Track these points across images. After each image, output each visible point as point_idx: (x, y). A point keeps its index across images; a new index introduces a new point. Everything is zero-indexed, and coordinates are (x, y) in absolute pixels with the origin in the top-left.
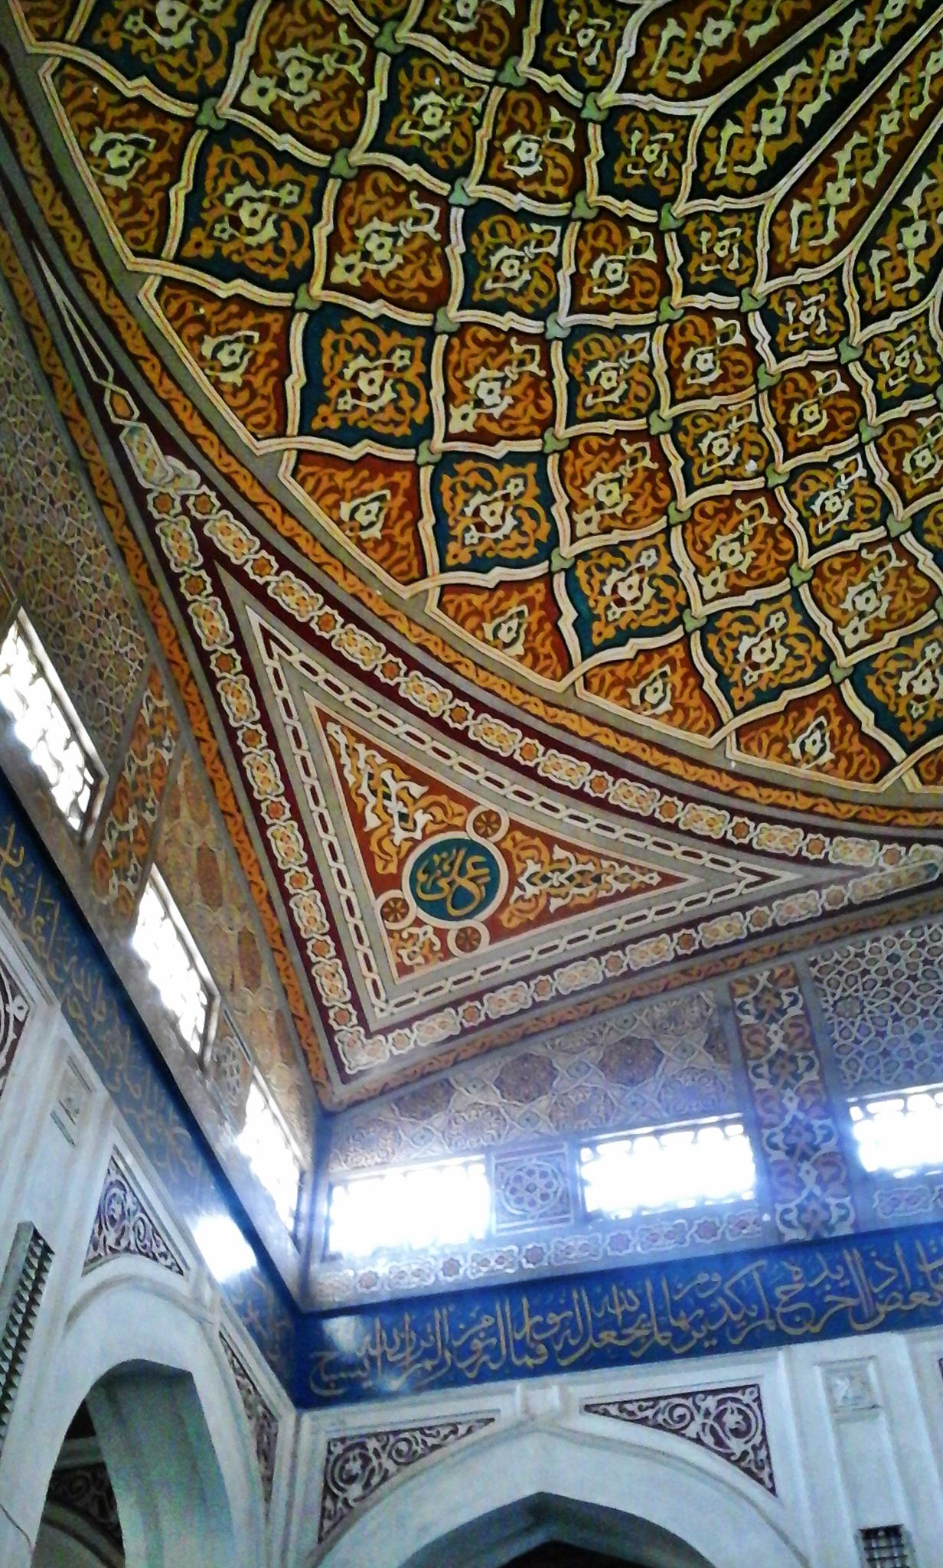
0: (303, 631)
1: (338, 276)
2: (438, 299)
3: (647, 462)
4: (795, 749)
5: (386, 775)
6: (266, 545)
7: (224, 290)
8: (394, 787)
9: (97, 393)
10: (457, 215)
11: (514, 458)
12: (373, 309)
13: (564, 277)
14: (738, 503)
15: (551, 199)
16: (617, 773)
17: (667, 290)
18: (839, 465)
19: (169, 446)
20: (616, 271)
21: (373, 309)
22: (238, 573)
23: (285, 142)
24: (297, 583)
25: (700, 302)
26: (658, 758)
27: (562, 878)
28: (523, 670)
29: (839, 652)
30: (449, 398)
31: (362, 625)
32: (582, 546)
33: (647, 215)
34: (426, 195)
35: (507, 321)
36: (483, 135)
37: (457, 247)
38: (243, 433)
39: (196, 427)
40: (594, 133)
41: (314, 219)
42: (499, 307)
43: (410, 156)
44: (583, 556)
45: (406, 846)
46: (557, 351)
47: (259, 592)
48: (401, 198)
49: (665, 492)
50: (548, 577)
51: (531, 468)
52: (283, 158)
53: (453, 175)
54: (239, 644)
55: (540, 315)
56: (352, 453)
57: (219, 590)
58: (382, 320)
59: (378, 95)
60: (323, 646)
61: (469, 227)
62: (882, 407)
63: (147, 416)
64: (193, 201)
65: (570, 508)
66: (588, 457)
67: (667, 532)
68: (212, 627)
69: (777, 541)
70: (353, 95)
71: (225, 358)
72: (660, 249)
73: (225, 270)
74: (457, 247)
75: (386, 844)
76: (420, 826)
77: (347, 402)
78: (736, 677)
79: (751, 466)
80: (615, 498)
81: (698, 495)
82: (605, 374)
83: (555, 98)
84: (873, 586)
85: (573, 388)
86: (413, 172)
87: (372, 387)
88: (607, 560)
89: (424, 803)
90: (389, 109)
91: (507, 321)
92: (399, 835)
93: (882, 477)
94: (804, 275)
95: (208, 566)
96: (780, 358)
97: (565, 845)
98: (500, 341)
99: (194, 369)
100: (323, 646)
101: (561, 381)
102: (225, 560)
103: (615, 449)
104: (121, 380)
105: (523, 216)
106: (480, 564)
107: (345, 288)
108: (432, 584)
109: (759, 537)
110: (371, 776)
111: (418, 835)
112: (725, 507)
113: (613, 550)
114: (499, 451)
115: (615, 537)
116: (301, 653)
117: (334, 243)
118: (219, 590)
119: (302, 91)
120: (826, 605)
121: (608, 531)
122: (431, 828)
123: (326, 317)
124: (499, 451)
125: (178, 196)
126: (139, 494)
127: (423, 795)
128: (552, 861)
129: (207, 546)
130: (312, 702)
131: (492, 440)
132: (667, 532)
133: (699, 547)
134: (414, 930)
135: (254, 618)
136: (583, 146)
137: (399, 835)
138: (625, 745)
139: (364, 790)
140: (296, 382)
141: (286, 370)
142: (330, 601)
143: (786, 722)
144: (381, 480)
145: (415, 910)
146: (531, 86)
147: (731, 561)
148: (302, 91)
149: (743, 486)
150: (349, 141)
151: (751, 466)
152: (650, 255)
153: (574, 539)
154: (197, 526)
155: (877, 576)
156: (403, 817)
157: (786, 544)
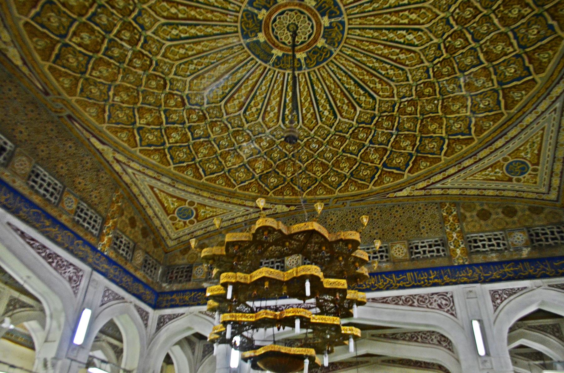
0: (444, 179)
2: (386, 150)
7: (376, 178)
8: (487, 173)
11: (420, 141)
12: (385, 158)
13: (386, 131)
15: (371, 132)
16: (505, 134)
17: (393, 115)
19: (401, 190)
21: (385, 158)
22: (428, 186)
23: (354, 167)
25: (396, 109)
26: (505, 126)
28: (469, 146)
32: (444, 132)
33: (377, 118)
34: (367, 149)
35: (392, 140)
36: (358, 141)
37: (377, 146)
40: (361, 125)
42: (389, 141)
43: (360, 151)
44: (446, 133)
47: (433, 183)
48: (367, 153)
50: (449, 139)
52: (357, 168)
54: (442, 189)
55: (392, 135)
56: (411, 165)
57: (431, 189)
58: (387, 157)
59: (349, 155)
60: (449, 176)
62: (429, 77)
63: (395, 192)
67: (446, 118)
68: (437, 192)
70: (348, 159)
73: (374, 177)
74: (377, 146)
80: (435, 126)
81: (439, 111)
82: (407, 126)
83: (353, 131)
85: (408, 131)
86: (362, 151)
87: (400, 160)
88: (449, 129)
90: (351, 153)
91: (392, 140)
93: (447, 78)
94: (395, 91)
96: (412, 96)
97: (521, 147)
98: (396, 141)
99: (390, 184)
100: (449, 176)
101: (406, 133)
103: (424, 125)
105: (373, 136)
108: (443, 157)
112: (444, 107)
113: (447, 127)
114: (418, 143)
115: (444, 127)
116: (449, 180)
117: (372, 163)
118: (431, 189)
119: (347, 165)
121: (442, 128)
123: (385, 165)
124: (418, 143)
125: (360, 182)
126: (408, 196)
130: (461, 180)
131: (415, 144)
132: (446, 118)
133: (453, 112)
135: (438, 185)
136: (363, 127)
138: (498, 132)
140: (395, 171)
141: (393, 172)
142: (440, 173)
145: (521, 177)
146: (351, 134)
147: (458, 107)
148: (347, 165)
149: (440, 103)
151: (436, 102)
154: (417, 190)
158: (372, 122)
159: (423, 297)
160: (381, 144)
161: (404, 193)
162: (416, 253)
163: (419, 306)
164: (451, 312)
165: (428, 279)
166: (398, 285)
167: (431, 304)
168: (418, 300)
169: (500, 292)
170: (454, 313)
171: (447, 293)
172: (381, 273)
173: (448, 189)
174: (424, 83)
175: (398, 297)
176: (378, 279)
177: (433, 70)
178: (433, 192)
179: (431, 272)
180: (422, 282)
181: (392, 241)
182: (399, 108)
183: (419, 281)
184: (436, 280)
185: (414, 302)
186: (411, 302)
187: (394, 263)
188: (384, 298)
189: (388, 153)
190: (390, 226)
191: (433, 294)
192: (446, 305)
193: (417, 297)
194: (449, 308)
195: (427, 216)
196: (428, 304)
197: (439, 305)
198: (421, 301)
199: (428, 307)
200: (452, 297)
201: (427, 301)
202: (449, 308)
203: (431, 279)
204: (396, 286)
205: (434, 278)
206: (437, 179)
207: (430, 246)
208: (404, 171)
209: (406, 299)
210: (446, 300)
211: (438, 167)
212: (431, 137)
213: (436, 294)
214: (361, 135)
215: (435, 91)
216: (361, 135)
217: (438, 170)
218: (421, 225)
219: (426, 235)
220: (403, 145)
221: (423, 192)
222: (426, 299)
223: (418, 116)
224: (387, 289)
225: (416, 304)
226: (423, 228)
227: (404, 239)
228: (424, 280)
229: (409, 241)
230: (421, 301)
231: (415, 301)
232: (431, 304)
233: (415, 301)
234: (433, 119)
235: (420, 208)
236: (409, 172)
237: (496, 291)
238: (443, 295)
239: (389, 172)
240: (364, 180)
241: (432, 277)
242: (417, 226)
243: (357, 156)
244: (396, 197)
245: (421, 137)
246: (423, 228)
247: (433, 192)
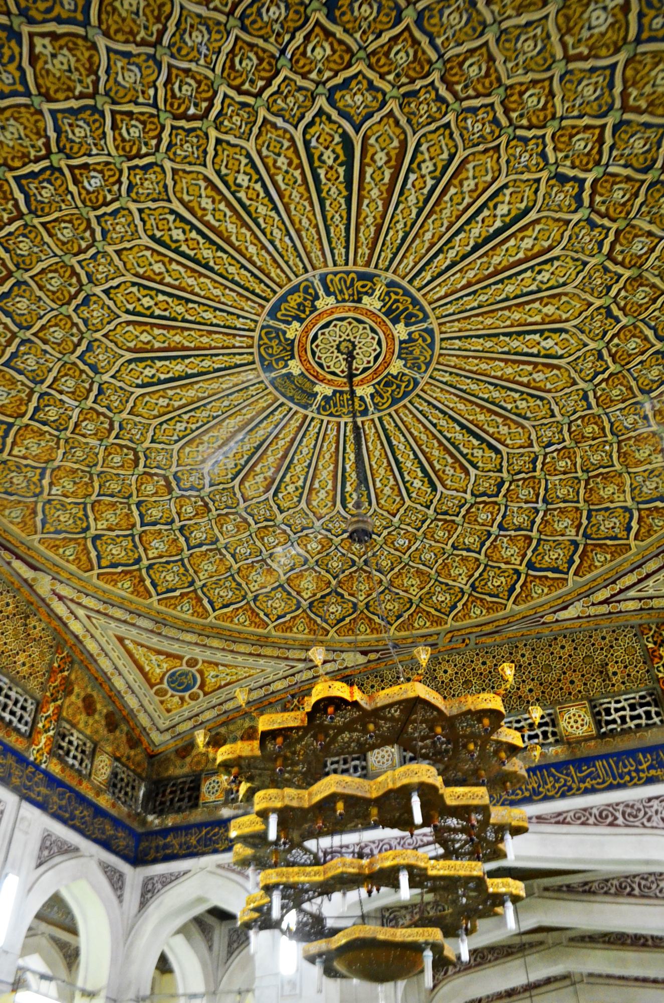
0: (640, 581)
1: (518, 562)
3: (599, 480)
6: (606, 587)
7: (518, 590)
9: (544, 623)
10: (502, 533)
11: (589, 517)
15: (499, 510)
17: (534, 477)
19: (565, 608)
20: (525, 492)
21: (529, 553)
22: (613, 596)
23: (477, 574)
24: (622, 580)
25: (539, 465)
30: (563, 535)
31: (644, 563)
33: (507, 485)
34: (495, 540)
35: (538, 520)
36: (478, 527)
37: (513, 533)
38: (564, 589)
39: (560, 601)
40: (479, 500)
41: (499, 568)
42: (533, 522)
43: (483, 544)
44: (633, 499)
46: (550, 507)
47: (621, 591)
49: (612, 474)
50: (639, 510)
51: (594, 513)
52: (481, 575)
53: (489, 534)
54: (640, 599)
55: (537, 511)
56: (577, 561)
57: (619, 602)
58: (533, 552)
59: (465, 553)
60: (648, 576)
61: (506, 530)
62: (590, 407)
63: (555, 612)
64: (491, 595)
65: (612, 502)
68: (632, 605)
70: (464, 559)
71: (540, 591)
72: (519, 480)
74: (513, 533)
77: (559, 562)
79: (607, 448)
80: (611, 489)
81: (616, 462)
82: (562, 492)
83: (468, 511)
85: (565, 501)
86: (488, 544)
88: (637, 492)
90: (468, 550)
91: (538, 520)
94: (533, 437)
95: (609, 604)
96: (564, 441)
98: (545, 522)
100: (648, 576)
101: (562, 505)
102: (607, 599)
103: (591, 489)
104: (542, 617)
105: (504, 517)
106: (629, 529)
107: (522, 561)
108: (633, 544)
113: (632, 490)
114: (585, 522)
115: (628, 489)
117: (507, 563)
118: (619, 602)
119: (463, 570)
121: (624, 491)
123: (530, 566)
124: (585, 522)
125: (489, 599)
126: (579, 617)
129: (601, 603)
131: (580, 524)
132: (629, 473)
133: (639, 463)
135: (632, 593)
136: (484, 502)
140: (550, 575)
141: (546, 577)
146: (464, 517)
147: (648, 452)
148: (463, 570)
149: (615, 449)
150: (477, 560)
151: (607, 448)
152: (520, 483)
153: (625, 501)
154: (593, 604)
158: (499, 491)
159: (632, 807)
160: (519, 529)
161: (571, 612)
162: (608, 723)
163: (627, 826)
165: (637, 771)
166: (582, 786)
167: (649, 820)
168: (624, 813)
172: (547, 767)
173: (651, 598)
174: (582, 418)
175: (585, 810)
176: (542, 776)
177: (595, 393)
178: (623, 606)
179: (641, 756)
180: (627, 778)
181: (560, 703)
182: (543, 464)
183: (622, 777)
184: (653, 772)
185: (616, 818)
186: (610, 819)
187: (569, 743)
188: (559, 814)
189: (534, 543)
190: (554, 675)
191: (650, 800)
193: (621, 808)
195: (619, 653)
196: (645, 820)
198: (629, 815)
199: (644, 826)
201: (642, 813)
203: (643, 771)
204: (579, 789)
205: (649, 768)
206: (628, 583)
207: (633, 707)
208: (567, 573)
209: (601, 813)
211: (625, 560)
212: (607, 509)
214: (482, 517)
215: (603, 429)
216: (482, 517)
217: (627, 566)
218: (611, 670)
219: (623, 687)
220: (559, 527)
221: (604, 609)
222: (639, 810)
223: (580, 474)
224: (563, 796)
225: (620, 821)
226: (615, 674)
227: (582, 699)
228: (629, 773)
229: (590, 701)
230: (629, 815)
231: (619, 815)
233: (619, 815)
234: (605, 476)
235: (604, 638)
236: (576, 574)
239: (540, 578)
240: (497, 596)
241: (645, 766)
242: (602, 670)
243: (479, 553)
244: (557, 621)
245: (590, 511)
246: (615, 674)
247: (623, 606)
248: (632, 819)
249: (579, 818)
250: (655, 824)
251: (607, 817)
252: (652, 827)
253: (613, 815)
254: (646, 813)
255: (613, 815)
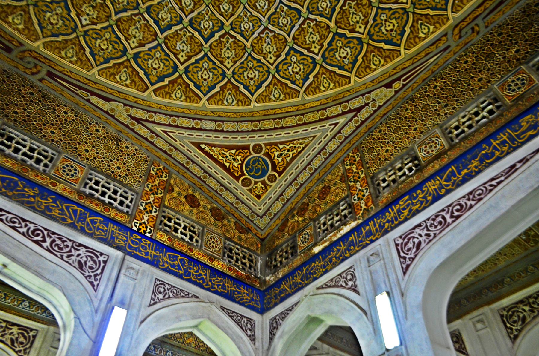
4: (322, 88)
5: (223, 152)
14: (261, 35)
18: (278, 10)
27: (286, 152)
29: (315, 56)
45: (239, 166)
66: (216, 48)
69: (278, 38)
75: (234, 168)
76: (239, 160)
78: (294, 79)
84: (311, 33)
89: (237, 154)
92: (236, 164)
109: (273, 40)
110: (220, 154)
111: (240, 162)
120: (302, 46)
122: (242, 159)
127: (235, 152)
128: (281, 150)
134: (256, 185)
137: (236, 164)
139: (221, 158)
143: (315, 82)
144: (176, 85)
155: (311, 30)
156: (234, 159)
157: (281, 37)
159: (64, 242)
164: (92, 279)
167: (68, 256)
169: (167, 286)
170: (96, 283)
171: (102, 254)
175: (24, 220)
185: (44, 241)
186: (39, 238)
192: (91, 268)
194: (92, 274)
197: (79, 262)
198: (57, 245)
200: (105, 262)
201: (68, 250)
202: (92, 274)
210: (95, 262)
213: (86, 247)
225: (46, 244)
231: (48, 240)
232: (68, 256)
233: (48, 240)
237: (163, 283)
238: (94, 253)
248: (56, 248)
249: (15, 222)
250: (71, 261)
251: (38, 235)
252: (67, 262)
253: (44, 237)
254: (70, 251)
255: (44, 237)
